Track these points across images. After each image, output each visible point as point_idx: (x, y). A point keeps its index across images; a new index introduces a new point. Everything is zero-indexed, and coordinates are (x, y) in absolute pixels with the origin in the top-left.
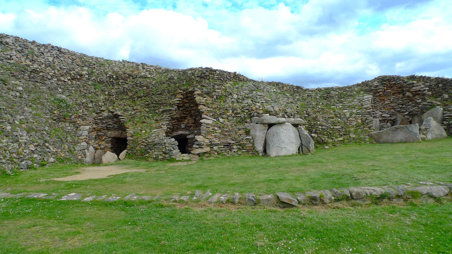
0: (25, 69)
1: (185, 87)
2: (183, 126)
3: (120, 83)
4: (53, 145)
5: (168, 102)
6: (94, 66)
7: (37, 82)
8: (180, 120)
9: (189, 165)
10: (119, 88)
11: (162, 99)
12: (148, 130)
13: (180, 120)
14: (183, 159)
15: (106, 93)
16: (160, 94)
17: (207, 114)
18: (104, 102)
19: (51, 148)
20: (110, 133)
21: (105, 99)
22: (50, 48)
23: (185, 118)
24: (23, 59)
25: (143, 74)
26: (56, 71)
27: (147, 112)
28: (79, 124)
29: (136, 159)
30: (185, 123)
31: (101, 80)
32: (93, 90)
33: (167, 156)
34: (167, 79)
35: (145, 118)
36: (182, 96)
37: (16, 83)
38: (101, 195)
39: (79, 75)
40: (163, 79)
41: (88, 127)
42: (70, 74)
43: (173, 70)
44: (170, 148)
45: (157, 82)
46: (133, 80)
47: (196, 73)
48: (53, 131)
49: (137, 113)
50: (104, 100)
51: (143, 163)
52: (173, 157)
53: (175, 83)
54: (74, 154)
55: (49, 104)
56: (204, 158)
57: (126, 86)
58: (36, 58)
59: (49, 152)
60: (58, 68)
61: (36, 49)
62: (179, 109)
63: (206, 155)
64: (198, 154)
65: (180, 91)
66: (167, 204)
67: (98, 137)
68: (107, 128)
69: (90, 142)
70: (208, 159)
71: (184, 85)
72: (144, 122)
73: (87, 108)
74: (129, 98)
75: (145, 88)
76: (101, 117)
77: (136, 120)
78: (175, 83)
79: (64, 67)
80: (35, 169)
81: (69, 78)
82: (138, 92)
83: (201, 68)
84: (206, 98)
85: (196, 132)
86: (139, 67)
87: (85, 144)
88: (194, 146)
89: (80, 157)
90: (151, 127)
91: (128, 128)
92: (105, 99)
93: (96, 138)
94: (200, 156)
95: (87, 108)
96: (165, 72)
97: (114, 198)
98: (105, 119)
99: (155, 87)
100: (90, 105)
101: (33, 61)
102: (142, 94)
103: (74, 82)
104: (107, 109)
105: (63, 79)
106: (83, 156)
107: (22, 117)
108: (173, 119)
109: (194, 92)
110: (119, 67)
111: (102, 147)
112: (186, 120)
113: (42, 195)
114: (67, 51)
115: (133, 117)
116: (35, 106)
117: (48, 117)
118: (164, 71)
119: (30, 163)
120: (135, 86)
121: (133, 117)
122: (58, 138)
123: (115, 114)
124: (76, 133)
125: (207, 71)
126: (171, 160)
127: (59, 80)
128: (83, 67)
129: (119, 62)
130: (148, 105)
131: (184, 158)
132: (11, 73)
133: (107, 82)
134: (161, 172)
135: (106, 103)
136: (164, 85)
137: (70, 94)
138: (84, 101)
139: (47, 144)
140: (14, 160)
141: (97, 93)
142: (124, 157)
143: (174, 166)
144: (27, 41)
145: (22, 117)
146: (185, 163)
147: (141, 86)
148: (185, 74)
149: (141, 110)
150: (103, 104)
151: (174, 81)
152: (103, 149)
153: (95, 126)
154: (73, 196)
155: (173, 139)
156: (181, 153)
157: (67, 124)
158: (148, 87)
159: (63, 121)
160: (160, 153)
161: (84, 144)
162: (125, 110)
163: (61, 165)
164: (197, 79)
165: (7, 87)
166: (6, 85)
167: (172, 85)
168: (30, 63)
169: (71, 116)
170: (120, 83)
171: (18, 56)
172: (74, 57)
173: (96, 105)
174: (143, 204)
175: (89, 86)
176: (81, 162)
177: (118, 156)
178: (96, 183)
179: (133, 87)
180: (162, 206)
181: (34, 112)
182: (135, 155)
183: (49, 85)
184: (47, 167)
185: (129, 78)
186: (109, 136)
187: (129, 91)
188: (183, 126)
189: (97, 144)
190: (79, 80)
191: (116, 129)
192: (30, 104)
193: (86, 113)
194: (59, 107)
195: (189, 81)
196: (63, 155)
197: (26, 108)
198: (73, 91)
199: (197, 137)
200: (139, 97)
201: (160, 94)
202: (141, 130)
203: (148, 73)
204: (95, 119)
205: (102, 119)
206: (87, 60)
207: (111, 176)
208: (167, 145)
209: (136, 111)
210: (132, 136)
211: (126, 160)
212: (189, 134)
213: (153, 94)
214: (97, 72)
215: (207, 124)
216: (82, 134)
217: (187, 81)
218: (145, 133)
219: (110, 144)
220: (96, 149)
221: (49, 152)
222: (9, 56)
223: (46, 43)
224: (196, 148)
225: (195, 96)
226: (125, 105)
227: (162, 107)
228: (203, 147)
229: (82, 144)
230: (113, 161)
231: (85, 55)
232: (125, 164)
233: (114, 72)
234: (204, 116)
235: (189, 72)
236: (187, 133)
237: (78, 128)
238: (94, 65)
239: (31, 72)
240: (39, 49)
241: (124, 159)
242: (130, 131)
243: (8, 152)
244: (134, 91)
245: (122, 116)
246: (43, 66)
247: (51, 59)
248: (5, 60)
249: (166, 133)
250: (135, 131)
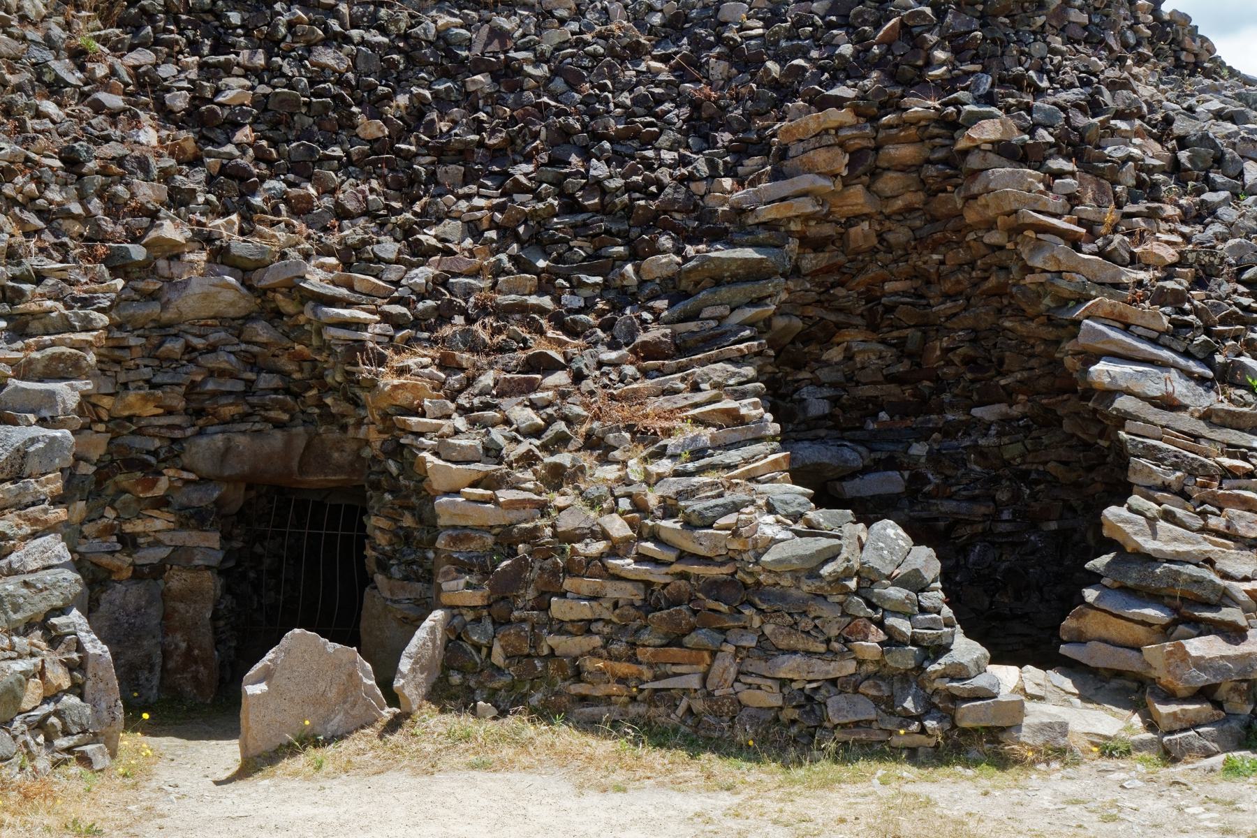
17: (1132, 313)
30: (824, 374)
85: (919, 449)
112: (835, 354)
152: (158, 571)
186: (206, 467)
200: (442, 153)
212: (865, 470)
225: (974, 161)
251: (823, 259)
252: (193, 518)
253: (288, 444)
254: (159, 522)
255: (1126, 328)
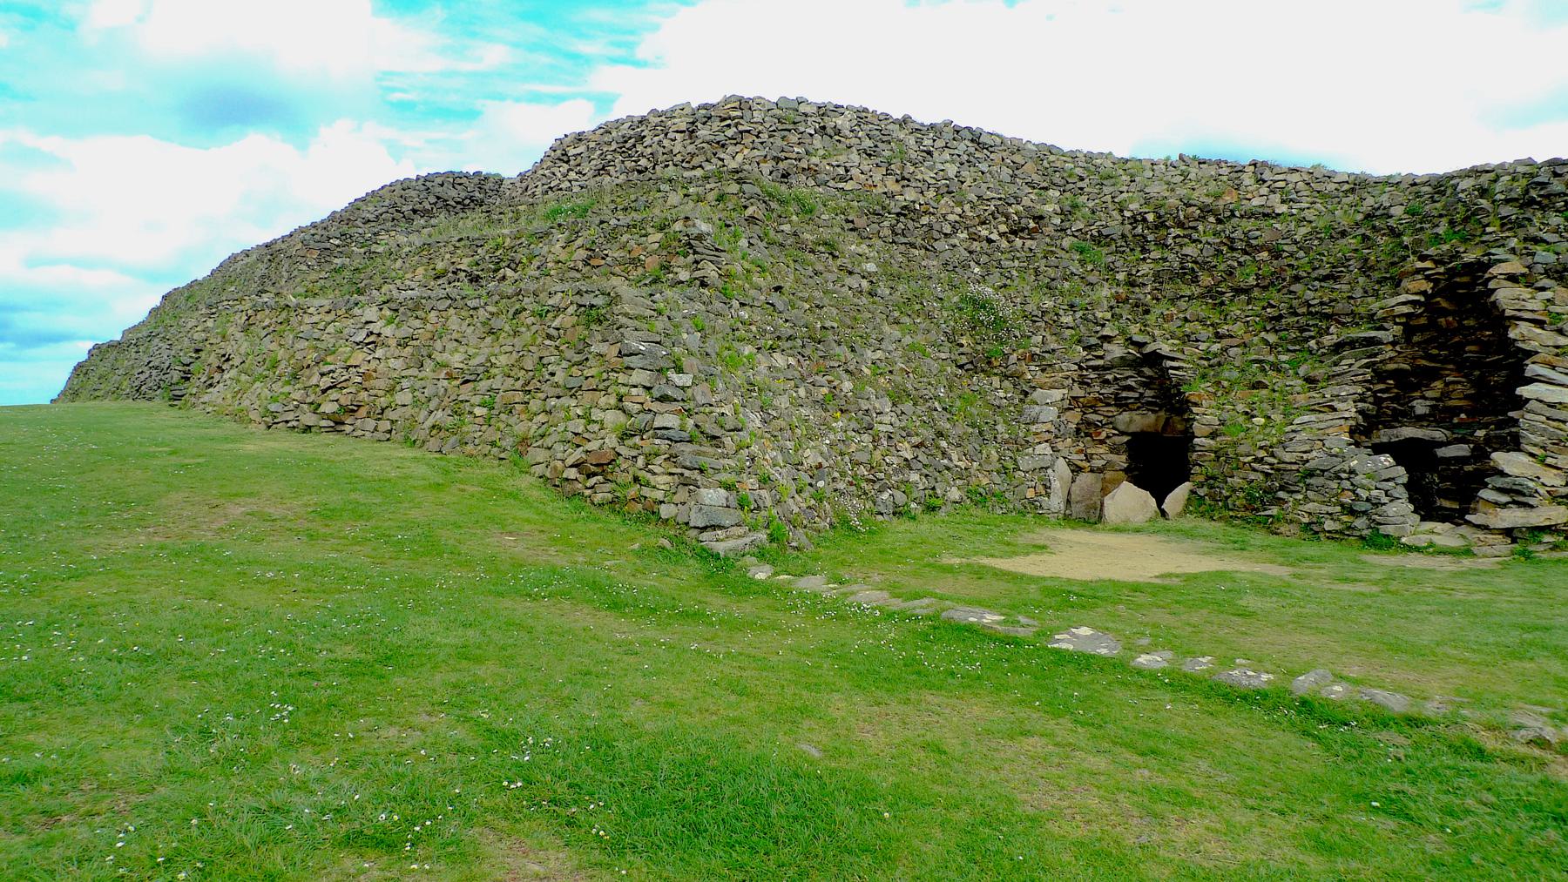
0: (884, 208)
1: (1446, 247)
2: (1421, 407)
3: (1170, 241)
4: (959, 445)
5: (1362, 310)
6: (1080, 184)
7: (913, 245)
8: (1408, 382)
9: (1470, 572)
10: (1165, 260)
11: (1334, 295)
12: (1277, 417)
13: (1408, 382)
14: (1431, 545)
15: (1121, 276)
16: (1325, 278)
18: (1112, 308)
19: (955, 457)
20: (1126, 416)
21: (1117, 297)
22: (948, 134)
23: (1434, 375)
24: (877, 177)
25: (1256, 202)
26: (967, 207)
27: (1272, 347)
28: (1029, 381)
29: (1229, 520)
30: (1429, 394)
31: (1105, 232)
32: (1075, 268)
33: (1360, 523)
34: (1360, 217)
35: (1263, 370)
36: (1428, 287)
37: (860, 250)
38: (1194, 655)
39: (1034, 218)
40: (1343, 219)
41: (1057, 394)
42: (1007, 217)
43: (1387, 182)
44: (1375, 493)
45: (1315, 231)
46: (1220, 227)
47: (1498, 187)
48: (958, 403)
49: (1232, 351)
50: (1113, 302)
51: (1258, 537)
52: (1390, 530)
53: (1394, 233)
54: (1015, 482)
55: (945, 314)
56: (1539, 551)
57: (1190, 250)
58: (912, 169)
59: (948, 469)
60: (972, 197)
61: (912, 141)
62: (1408, 341)
63: (1547, 538)
64: (1508, 532)
65: (1420, 265)
66: (1499, 746)
67: (1085, 430)
68: (1116, 399)
69: (1060, 446)
70: (1557, 555)
71: (1437, 239)
72: (1258, 385)
73: (1056, 326)
74: (1202, 296)
75: (1265, 254)
76: (1101, 362)
77: (1226, 374)
78: (1394, 233)
79: (990, 194)
80: (914, 518)
81: (1003, 228)
82: (1237, 273)
83: (1530, 163)
84: (1548, 294)
85: (1481, 433)
86: (1244, 176)
87: (1049, 451)
88: (1484, 493)
89: (1030, 494)
90: (1287, 404)
91: (1196, 405)
92: (1117, 297)
93: (1078, 431)
94: (1514, 541)
95: (1056, 326)
96: (1352, 190)
97: (1244, 675)
98: (1113, 367)
99: (1307, 251)
100: (1067, 319)
101: (904, 178)
102: (1252, 281)
103: (1018, 242)
104: (1123, 332)
105: (984, 233)
106: (1041, 489)
107: (879, 354)
108: (1380, 376)
109: (1490, 264)
110: (1168, 183)
111: (1098, 463)
112: (1439, 384)
113: (989, 618)
114: (998, 141)
115: (1214, 363)
116: (907, 320)
117: (943, 356)
118: (1346, 187)
119: (900, 498)
120: (1225, 249)
121: (1214, 363)
122: (973, 425)
123: (1148, 350)
124: (1021, 413)
125: (1556, 175)
126: (1378, 540)
127: (974, 238)
128: (1046, 189)
129: (1168, 164)
130: (1279, 318)
131: (1436, 539)
132: (847, 221)
133: (1123, 236)
134: (1360, 588)
135: (1117, 311)
136: (1344, 241)
137: (1004, 281)
138: (1049, 304)
139: (944, 444)
140: (863, 485)
141: (1092, 278)
142: (1180, 508)
143: (1403, 570)
144: (887, 117)
145: (879, 354)
146: (1445, 564)
147: (1250, 250)
148: (1443, 193)
149: (1247, 338)
150: (1108, 315)
151: (1391, 222)
152: (1100, 470)
153: (1078, 391)
154: (1079, 637)
155: (1386, 460)
156: (1417, 517)
157: (996, 381)
158: (1276, 254)
159: (983, 371)
160: (1330, 509)
161: (1044, 449)
162: (1187, 339)
163: (979, 512)
164: (1505, 210)
165: (839, 262)
166: (835, 257)
167: (1382, 240)
168: (897, 188)
169: (1006, 356)
170: (1170, 241)
171: (866, 168)
172: (1018, 158)
173: (1084, 318)
174: (1386, 725)
175: (1061, 254)
176: (1033, 508)
177: (1160, 502)
178: (1140, 598)
179: (1219, 252)
180: (1480, 753)
181: (907, 340)
182: (1226, 507)
183: (947, 255)
184: (942, 514)
185: (1202, 218)
186: (1122, 428)
187: (1202, 269)
188: (1421, 407)
189: (1081, 451)
190: (1032, 233)
191: (1149, 403)
192: (896, 314)
193: (1054, 346)
194: (974, 325)
195: (1466, 220)
196: (985, 481)
197: (886, 328)
198: (1014, 273)
199: (1500, 459)
200: (1238, 291)
201: (1325, 278)
202: (1249, 416)
203: (1276, 198)
204: (1081, 368)
205: (1104, 368)
206: (1058, 164)
207: (1170, 575)
208: (1358, 479)
209: (1226, 342)
210: (1213, 435)
211: (1190, 522)
213: (1297, 279)
214: (1091, 204)
215: (1551, 406)
216: (1038, 415)
217: (1452, 223)
218: (1265, 426)
219: (1124, 457)
220: (1077, 470)
221: (948, 469)
222: (841, 171)
223: (938, 119)
224: (1496, 504)
225: (1491, 285)
226: (1186, 320)
227: (1332, 329)
228: (1531, 501)
229: (1040, 449)
230: (1139, 519)
231: (1051, 150)
232: (1188, 534)
233: (1147, 202)
234: (1532, 369)
235: (1466, 184)
236: (1439, 434)
237: (1026, 394)
238: (1082, 179)
239: (898, 214)
240: (919, 142)
241: (1180, 515)
242: (1205, 416)
243: (847, 458)
244: (1222, 267)
245: (1173, 359)
246: (931, 194)
247: (952, 170)
248: (831, 183)
249: (1352, 432)
250: (1226, 416)
251: (1427, 335)
252: (1114, 450)
253: (1157, 419)
254: (1102, 449)
255: (1553, 368)
